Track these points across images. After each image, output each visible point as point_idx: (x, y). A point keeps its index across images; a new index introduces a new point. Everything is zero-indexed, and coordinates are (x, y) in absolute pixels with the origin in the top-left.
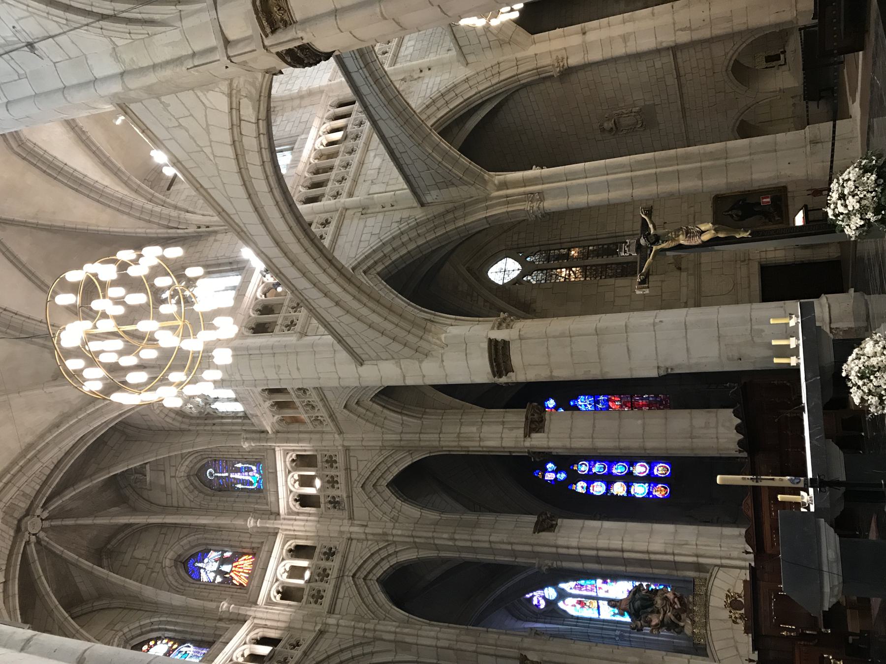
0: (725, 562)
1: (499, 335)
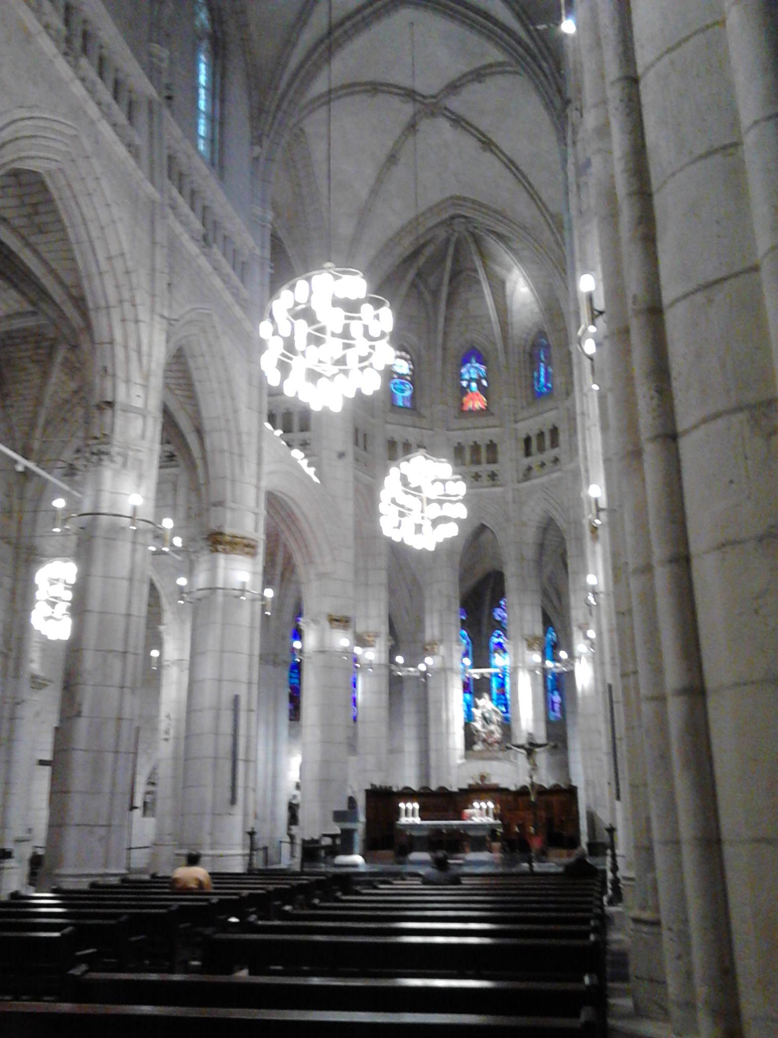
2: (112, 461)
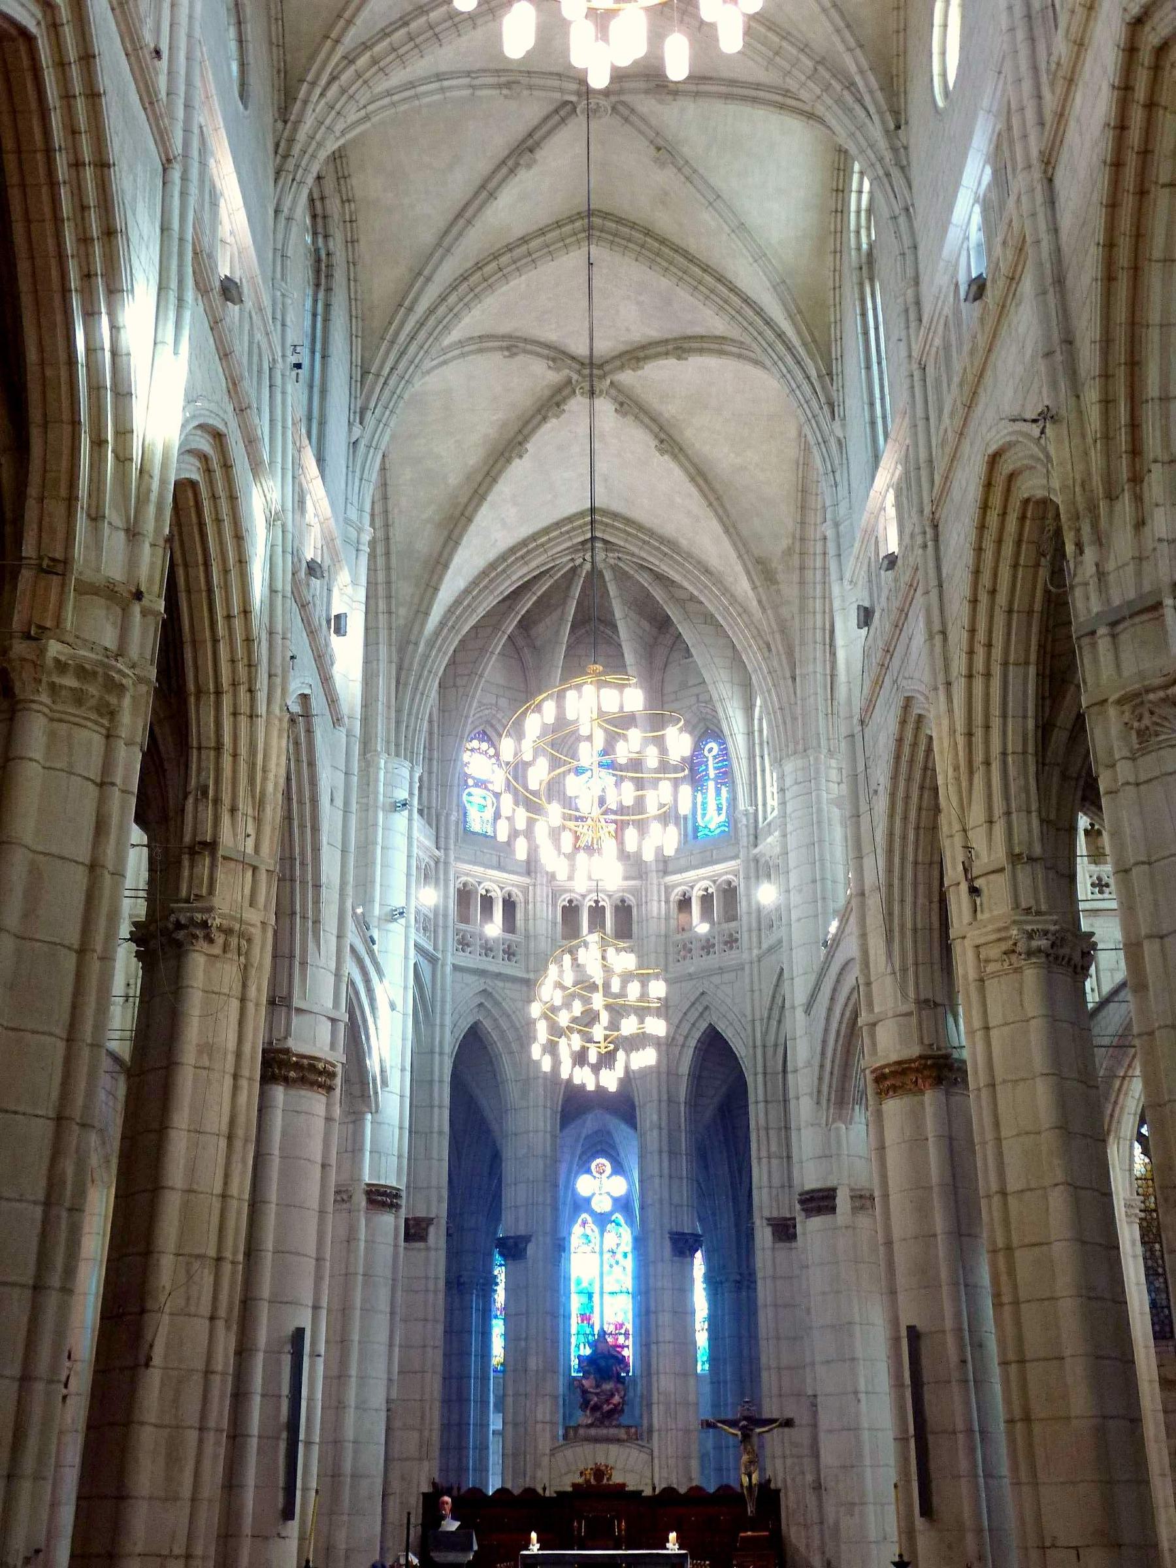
0: (656, 1461)
1: (843, 1201)
2: (211, 941)
